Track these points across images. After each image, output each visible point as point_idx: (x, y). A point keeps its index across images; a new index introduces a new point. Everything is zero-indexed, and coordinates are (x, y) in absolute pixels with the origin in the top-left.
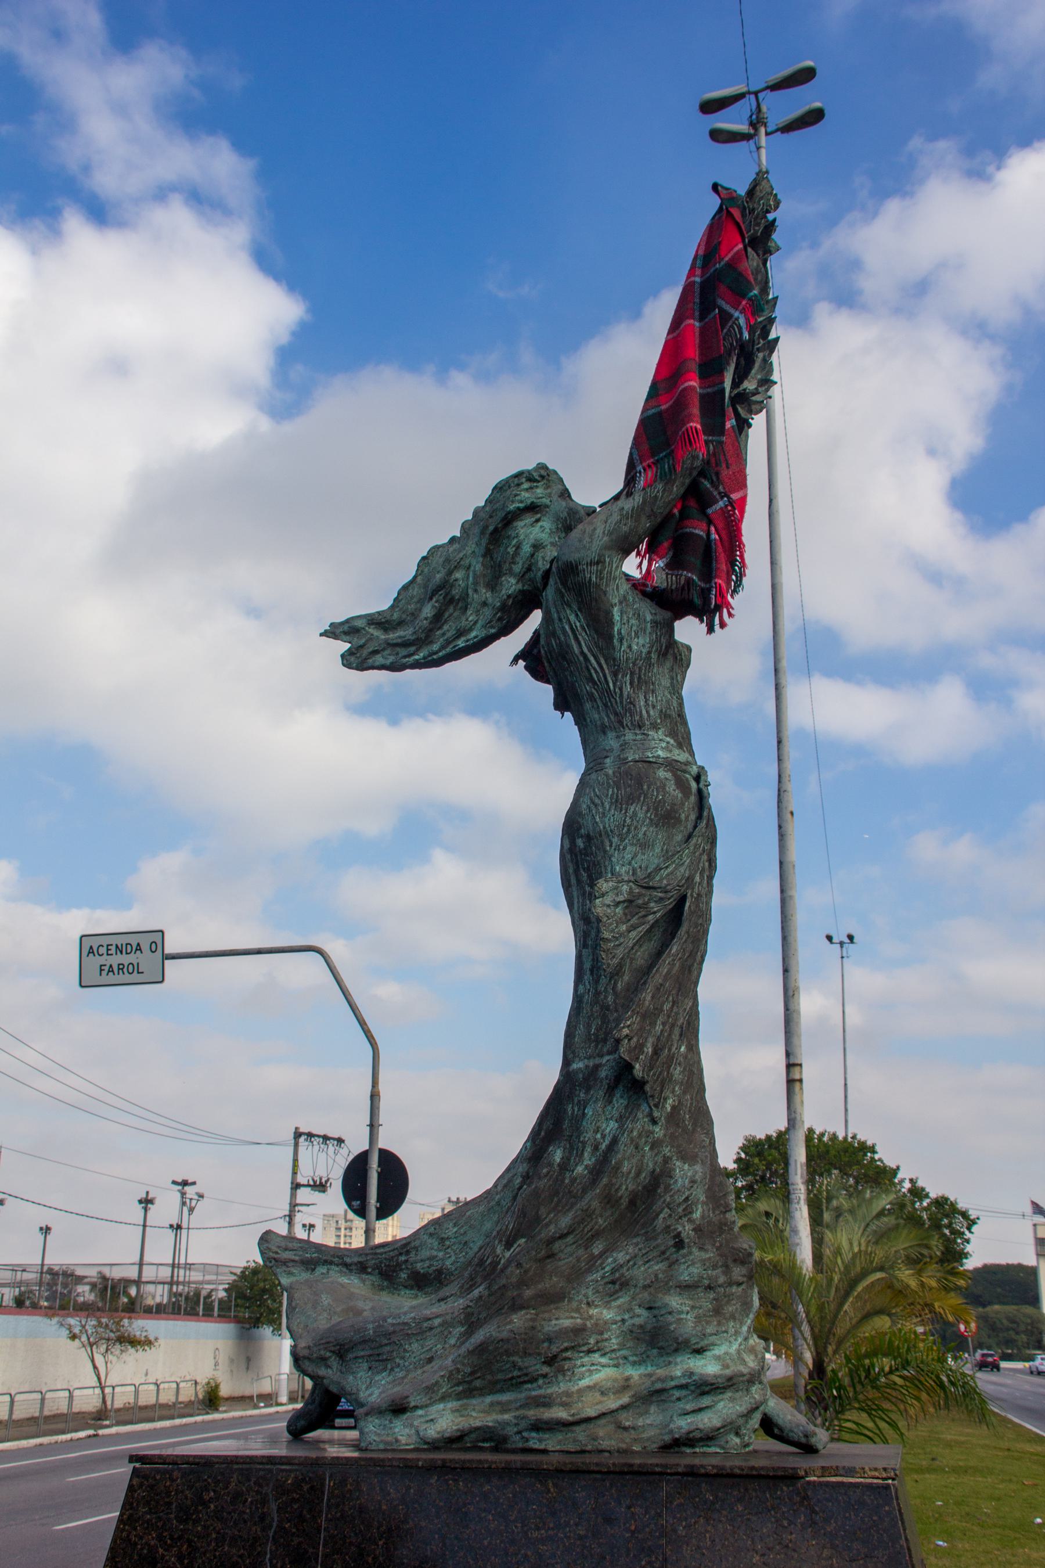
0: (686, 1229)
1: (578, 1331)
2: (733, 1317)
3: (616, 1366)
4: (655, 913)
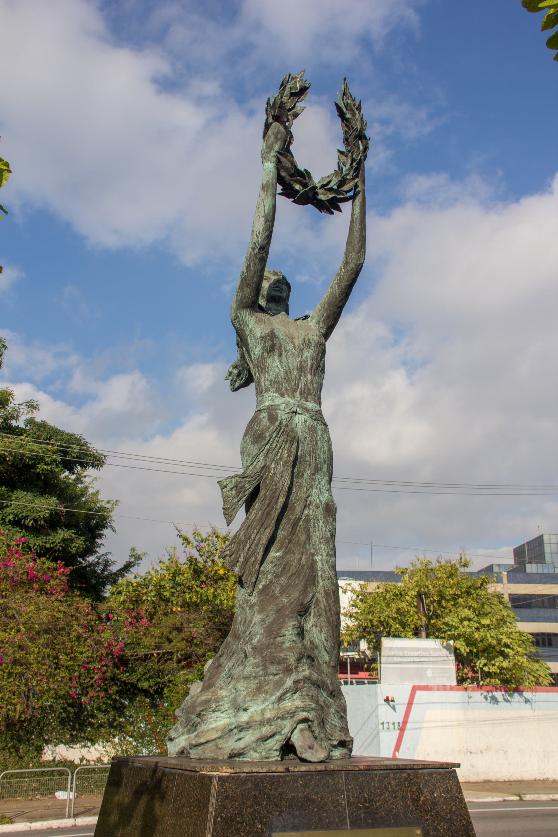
0: (248, 648)
1: (207, 702)
2: (266, 692)
3: (229, 718)
4: (248, 489)
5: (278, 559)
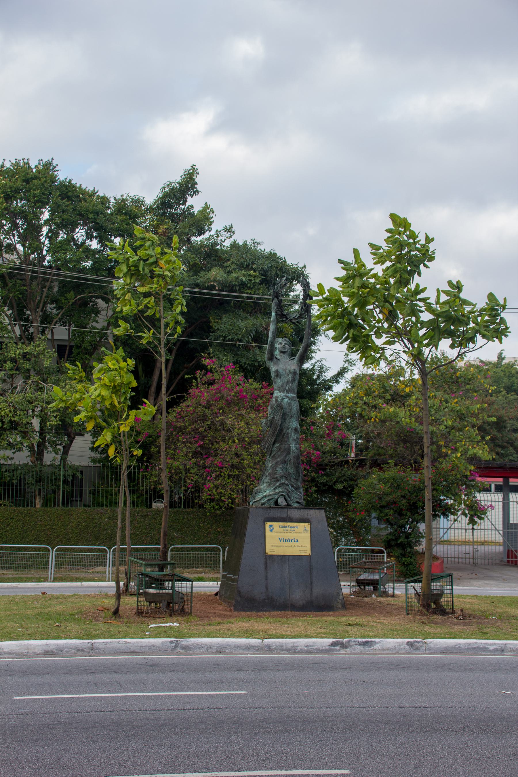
5: (278, 446)
